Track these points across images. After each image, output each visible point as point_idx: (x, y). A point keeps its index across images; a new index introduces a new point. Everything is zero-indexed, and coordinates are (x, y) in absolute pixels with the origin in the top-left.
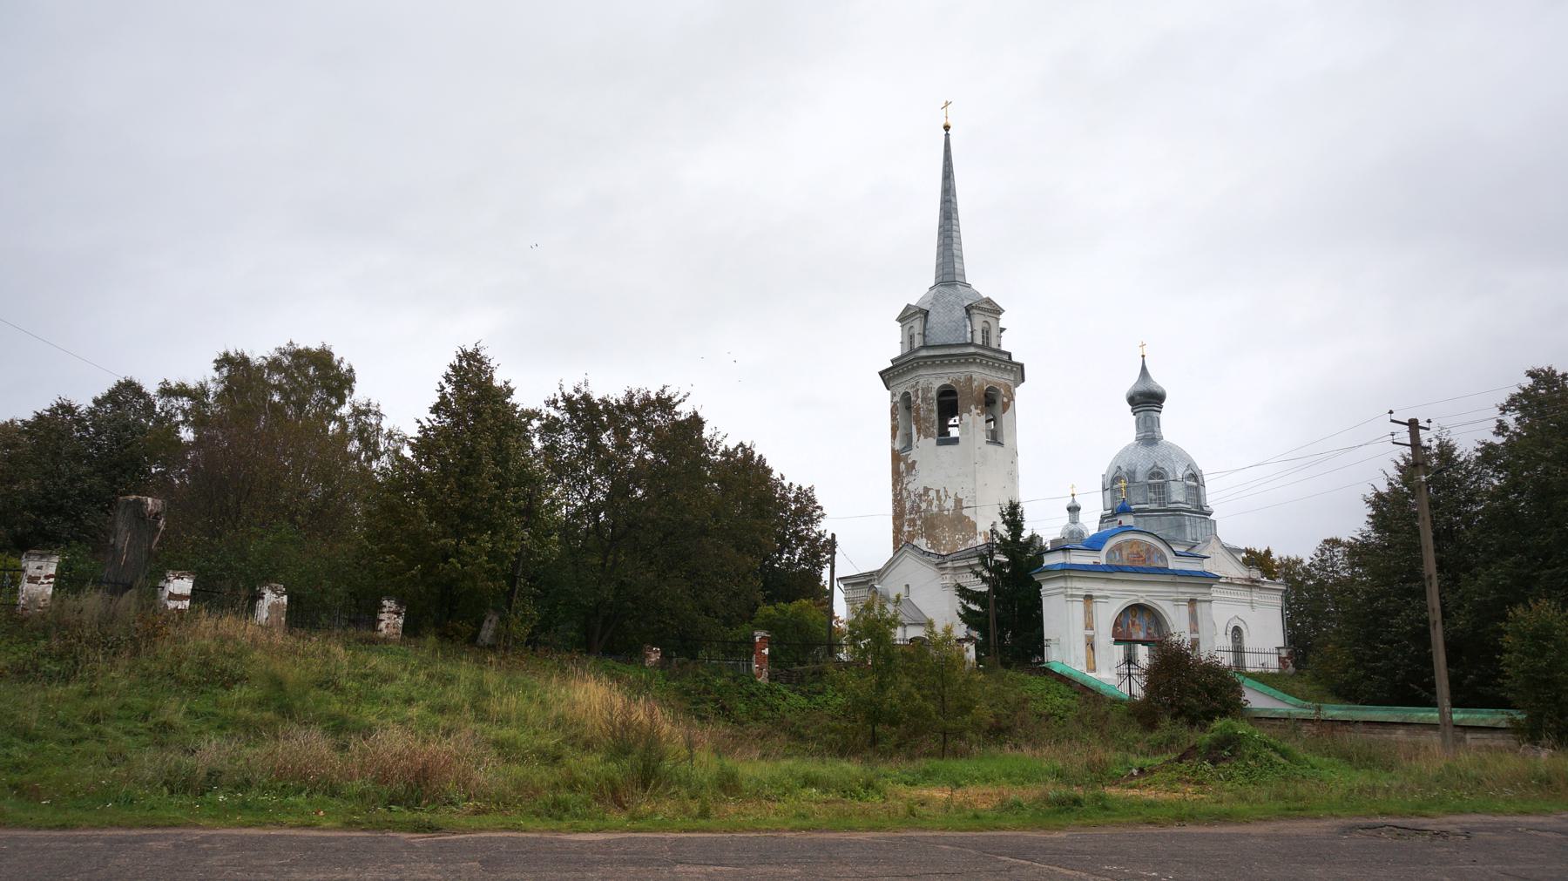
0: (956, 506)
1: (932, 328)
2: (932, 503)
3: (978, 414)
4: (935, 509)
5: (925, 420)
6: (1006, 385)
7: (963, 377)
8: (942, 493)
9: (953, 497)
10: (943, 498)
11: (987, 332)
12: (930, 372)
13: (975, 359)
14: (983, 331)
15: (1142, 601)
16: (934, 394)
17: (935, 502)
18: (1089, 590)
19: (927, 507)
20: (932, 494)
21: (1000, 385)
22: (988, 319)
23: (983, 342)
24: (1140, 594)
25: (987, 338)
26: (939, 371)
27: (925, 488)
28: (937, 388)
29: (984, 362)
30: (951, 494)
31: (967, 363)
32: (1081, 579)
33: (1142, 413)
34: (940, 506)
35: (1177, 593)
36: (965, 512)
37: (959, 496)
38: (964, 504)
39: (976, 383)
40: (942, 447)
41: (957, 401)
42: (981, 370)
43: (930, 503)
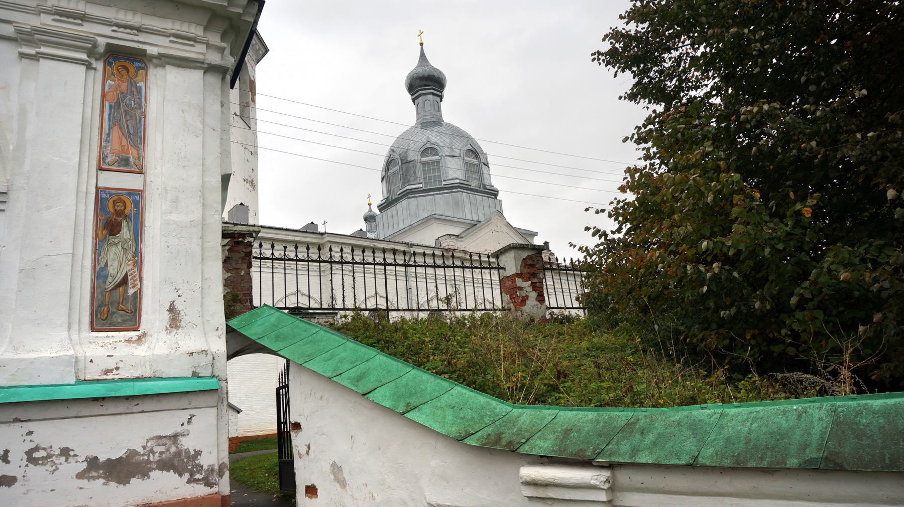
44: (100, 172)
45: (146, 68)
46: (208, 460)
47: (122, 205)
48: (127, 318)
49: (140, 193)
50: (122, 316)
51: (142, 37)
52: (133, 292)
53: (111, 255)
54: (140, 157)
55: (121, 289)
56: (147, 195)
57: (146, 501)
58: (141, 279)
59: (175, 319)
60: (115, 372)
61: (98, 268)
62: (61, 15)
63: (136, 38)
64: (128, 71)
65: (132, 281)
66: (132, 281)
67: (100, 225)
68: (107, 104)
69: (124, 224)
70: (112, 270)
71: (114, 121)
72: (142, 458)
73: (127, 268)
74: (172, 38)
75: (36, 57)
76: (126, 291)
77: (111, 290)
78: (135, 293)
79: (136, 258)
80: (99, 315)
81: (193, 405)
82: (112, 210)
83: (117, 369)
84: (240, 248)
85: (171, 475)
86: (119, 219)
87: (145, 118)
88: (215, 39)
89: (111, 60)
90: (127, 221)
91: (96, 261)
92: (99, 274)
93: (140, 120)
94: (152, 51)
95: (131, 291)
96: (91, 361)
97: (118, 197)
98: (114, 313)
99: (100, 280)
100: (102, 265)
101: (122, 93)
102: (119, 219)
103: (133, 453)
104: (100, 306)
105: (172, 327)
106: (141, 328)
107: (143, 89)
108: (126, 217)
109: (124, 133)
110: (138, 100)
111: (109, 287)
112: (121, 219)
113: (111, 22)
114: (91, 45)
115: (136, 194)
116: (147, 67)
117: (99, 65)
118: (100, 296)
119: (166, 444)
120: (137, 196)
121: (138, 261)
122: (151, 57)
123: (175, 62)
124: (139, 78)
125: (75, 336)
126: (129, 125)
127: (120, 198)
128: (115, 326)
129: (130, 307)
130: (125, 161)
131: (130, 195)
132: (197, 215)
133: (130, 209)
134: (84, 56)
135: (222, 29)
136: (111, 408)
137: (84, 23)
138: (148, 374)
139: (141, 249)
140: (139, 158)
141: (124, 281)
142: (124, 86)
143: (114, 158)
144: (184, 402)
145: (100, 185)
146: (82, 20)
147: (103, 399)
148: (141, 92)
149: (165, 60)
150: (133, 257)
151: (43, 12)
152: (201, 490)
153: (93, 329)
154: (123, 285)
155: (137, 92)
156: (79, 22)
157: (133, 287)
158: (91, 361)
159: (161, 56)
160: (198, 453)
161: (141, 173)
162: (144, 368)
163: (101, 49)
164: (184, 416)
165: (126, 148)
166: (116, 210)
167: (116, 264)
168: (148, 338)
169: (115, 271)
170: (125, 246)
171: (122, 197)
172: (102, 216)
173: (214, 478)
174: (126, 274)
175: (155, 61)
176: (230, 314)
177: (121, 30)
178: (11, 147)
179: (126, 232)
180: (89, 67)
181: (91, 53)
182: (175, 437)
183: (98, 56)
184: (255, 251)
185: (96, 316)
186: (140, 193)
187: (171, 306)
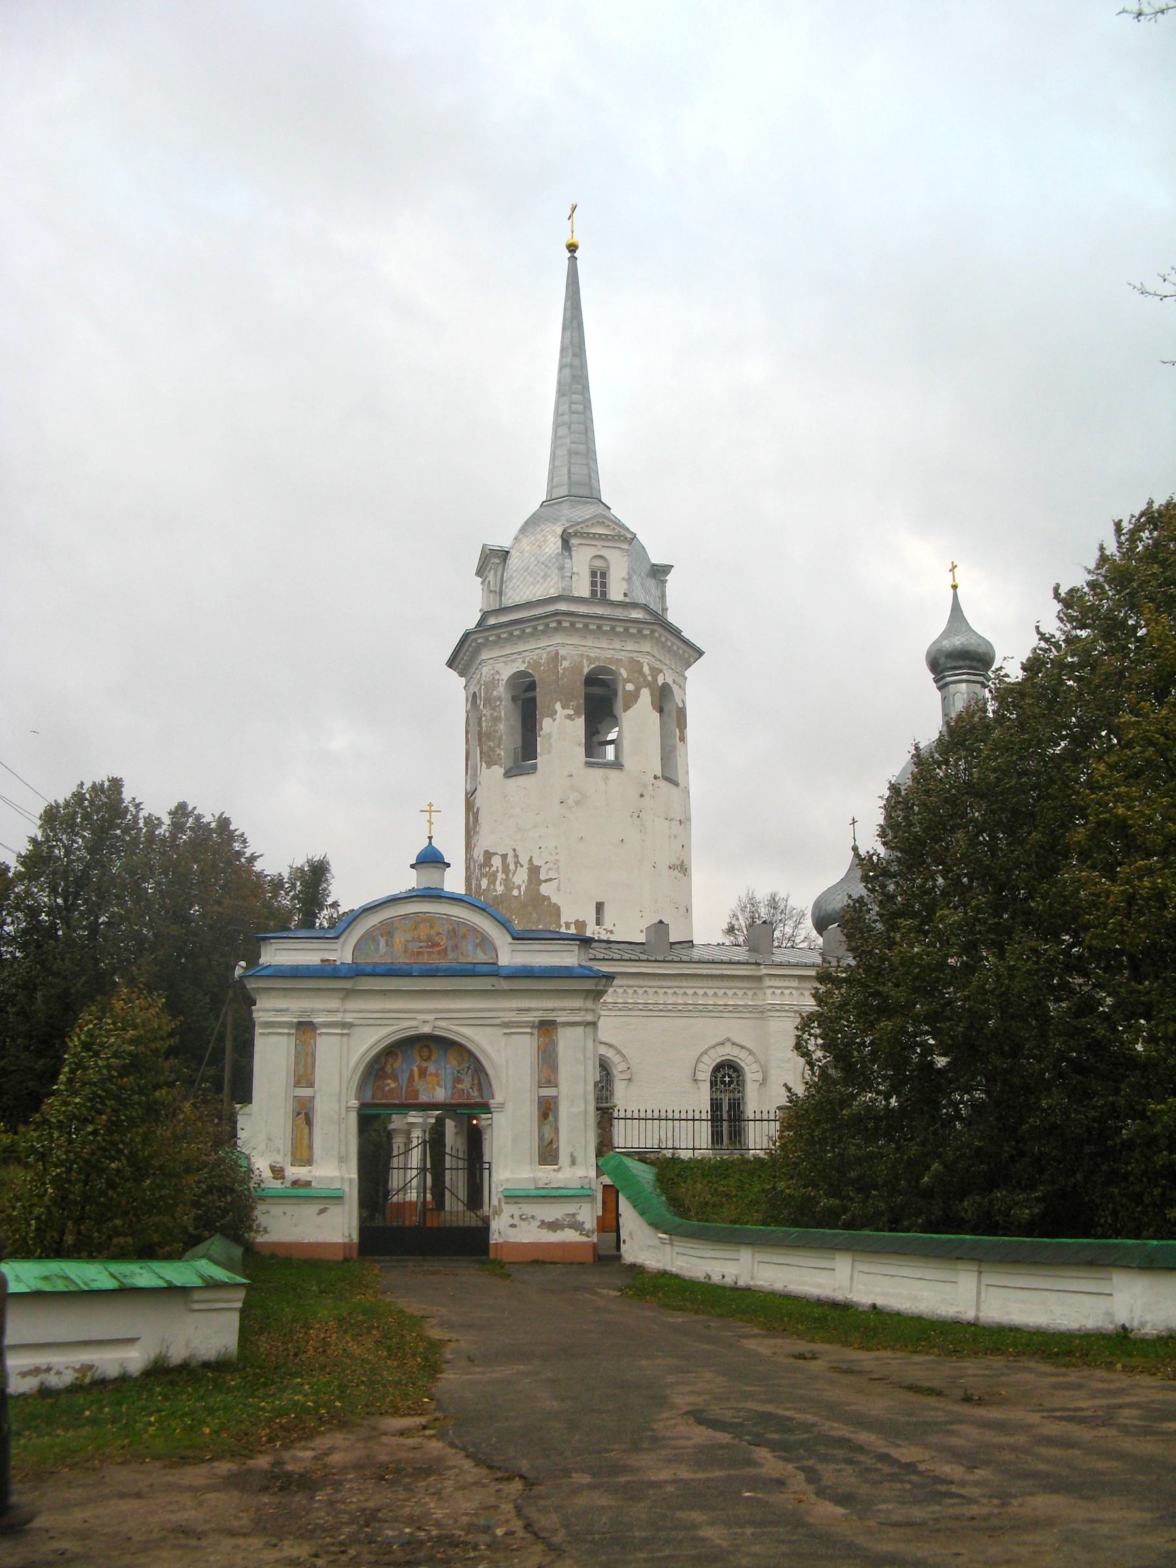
0: (530, 880)
1: (511, 578)
2: (495, 878)
3: (569, 717)
4: (500, 889)
5: (489, 736)
6: (632, 660)
7: (545, 656)
8: (510, 859)
9: (526, 865)
10: (512, 867)
11: (603, 575)
13: (559, 622)
14: (593, 574)
15: (427, 1029)
16: (501, 690)
17: (501, 876)
19: (489, 885)
20: (496, 862)
21: (618, 661)
22: (604, 552)
23: (594, 593)
24: (419, 1016)
25: (604, 585)
27: (487, 852)
28: (506, 679)
29: (541, 628)
30: (524, 860)
31: (547, 631)
33: (964, 685)
34: (507, 883)
36: (544, 889)
37: (536, 862)
38: (543, 876)
39: (566, 664)
40: (514, 779)
41: (534, 699)
42: (575, 640)
43: (492, 878)
46: (588, 1226)
70: (546, 1136)
73: (552, 1135)
84: (606, 1115)
85: (573, 1230)
92: (541, 1138)
103: (557, 1220)
106: (560, 1163)
132: (582, 1108)
133: (553, 1106)
136: (548, 1200)
141: (551, 1142)
144: (577, 1200)
152: (585, 1239)
160: (583, 1223)
164: (578, 1206)
173: (590, 1234)
176: (599, 1154)
179: (551, 1118)
182: (574, 1215)
184: (615, 1115)
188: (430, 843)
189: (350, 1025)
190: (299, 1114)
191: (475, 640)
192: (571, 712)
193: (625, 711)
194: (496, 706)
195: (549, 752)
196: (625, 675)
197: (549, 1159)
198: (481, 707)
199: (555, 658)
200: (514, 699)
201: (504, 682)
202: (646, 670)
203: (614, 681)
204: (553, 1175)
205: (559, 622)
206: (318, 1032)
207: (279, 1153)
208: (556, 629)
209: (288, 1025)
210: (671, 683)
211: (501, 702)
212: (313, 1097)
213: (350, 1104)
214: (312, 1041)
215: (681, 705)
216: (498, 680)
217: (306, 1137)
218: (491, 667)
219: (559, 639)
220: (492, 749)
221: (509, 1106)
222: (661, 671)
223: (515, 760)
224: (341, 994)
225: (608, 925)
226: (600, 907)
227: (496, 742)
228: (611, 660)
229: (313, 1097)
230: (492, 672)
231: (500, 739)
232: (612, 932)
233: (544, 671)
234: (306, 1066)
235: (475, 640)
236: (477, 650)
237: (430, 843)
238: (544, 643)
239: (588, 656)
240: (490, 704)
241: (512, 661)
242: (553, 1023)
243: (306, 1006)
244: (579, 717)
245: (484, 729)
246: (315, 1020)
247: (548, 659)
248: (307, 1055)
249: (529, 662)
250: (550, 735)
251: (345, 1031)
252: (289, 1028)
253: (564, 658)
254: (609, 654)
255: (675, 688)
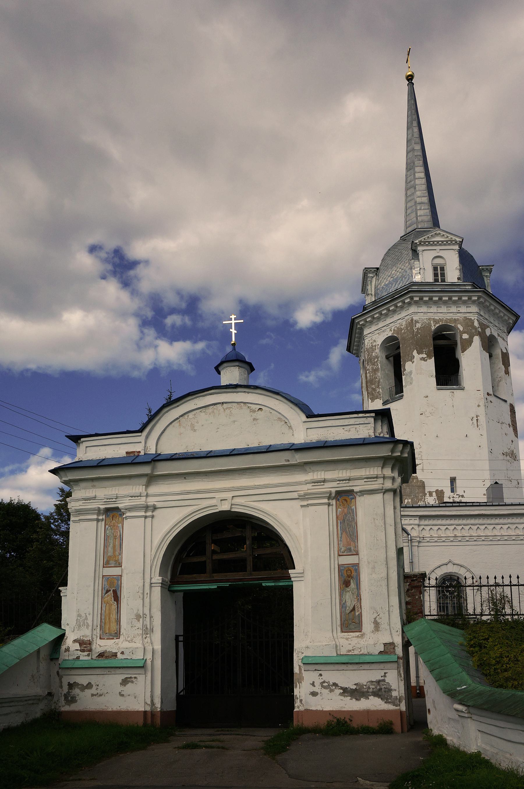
3: (423, 359)
6: (466, 319)
7: (404, 323)
12: (374, 328)
13: (412, 298)
15: (225, 507)
18: (109, 499)
21: (455, 321)
26: (381, 324)
31: (405, 306)
32: (96, 483)
35: (307, 483)
39: (418, 325)
42: (424, 309)
44: (339, 557)
45: (355, 498)
47: (350, 572)
48: (356, 626)
49: (357, 565)
50: (354, 625)
51: (351, 483)
52: (358, 614)
53: (347, 597)
54: (356, 547)
55: (353, 612)
56: (360, 565)
57: (368, 709)
58: (361, 606)
59: (377, 625)
60: (352, 651)
61: (342, 603)
62: (315, 483)
63: (348, 485)
64: (347, 501)
65: (357, 608)
66: (357, 608)
67: (342, 583)
68: (339, 521)
69: (352, 581)
70: (348, 604)
71: (343, 530)
72: (365, 690)
73: (354, 603)
74: (365, 480)
75: (308, 505)
76: (355, 614)
77: (348, 613)
78: (359, 614)
79: (358, 598)
80: (344, 625)
81: (386, 668)
82: (346, 575)
83: (353, 650)
86: (349, 579)
87: (357, 525)
88: (388, 472)
89: (339, 498)
90: (352, 580)
91: (341, 600)
92: (343, 605)
93: (354, 526)
94: (356, 489)
95: (357, 614)
96: (342, 646)
97: (347, 568)
98: (351, 624)
99: (344, 609)
100: (344, 602)
101: (345, 514)
102: (349, 579)
104: (344, 621)
105: (376, 631)
107: (355, 510)
108: (352, 577)
109: (348, 535)
110: (353, 516)
111: (348, 612)
112: (350, 579)
113: (336, 480)
114: (329, 495)
115: (355, 566)
116: (356, 497)
117: (334, 502)
118: (344, 617)
119: (375, 685)
120: (356, 567)
121: (359, 599)
122: (357, 493)
123: (367, 492)
124: (352, 504)
125: (335, 635)
126: (350, 530)
127: (349, 569)
128: (351, 630)
129: (357, 621)
130: (350, 550)
131: (353, 566)
133: (354, 574)
134: (326, 501)
135: (391, 465)
137: (325, 484)
138: (366, 653)
139: (360, 593)
140: (356, 548)
141: (354, 609)
142: (346, 510)
143: (344, 548)
145: (340, 563)
146: (323, 482)
147: (347, 663)
148: (354, 512)
149: (363, 493)
150: (357, 597)
151: (307, 483)
153: (342, 632)
154: (353, 610)
155: (352, 512)
156: (323, 484)
157: (358, 611)
158: (342, 646)
159: (360, 492)
161: (357, 554)
162: (364, 650)
163: (333, 495)
165: (349, 543)
166: (347, 575)
167: (349, 601)
168: (366, 636)
169: (350, 604)
170: (353, 592)
171: (350, 568)
172: (342, 578)
174: (354, 605)
175: (358, 494)
177: (341, 482)
178: (303, 551)
179: (353, 585)
180: (329, 505)
181: (329, 498)
183: (332, 498)
185: (343, 625)
186: (357, 565)
187: (374, 620)
188: (234, 349)
189: (155, 508)
190: (108, 591)
191: (358, 323)
192: (424, 356)
193: (463, 352)
194: (375, 362)
195: (411, 383)
196: (461, 328)
197: (352, 626)
198: (366, 366)
199: (412, 323)
200: (387, 358)
201: (379, 346)
202: (476, 324)
203: (454, 335)
204: (354, 641)
205: (412, 298)
206: (124, 516)
207: (87, 628)
208: (409, 304)
209: (99, 511)
210: (496, 336)
211: (378, 358)
212: (121, 576)
213: (153, 581)
214: (120, 525)
215: (505, 351)
216: (375, 346)
217: (114, 612)
218: (370, 339)
219: (413, 309)
220: (374, 390)
221: (308, 575)
222: (488, 327)
223: (391, 395)
224: (144, 480)
225: (459, 491)
226: (453, 480)
227: (377, 384)
228: (450, 320)
229: (121, 576)
230: (371, 341)
231: (379, 382)
232: (463, 496)
233: (404, 333)
234: (114, 547)
235: (358, 323)
236: (362, 330)
237: (234, 349)
238: (404, 314)
239: (434, 319)
240: (371, 362)
241: (383, 331)
242: (349, 493)
243: (113, 493)
244: (430, 358)
245: (368, 378)
246: (120, 506)
247: (406, 325)
248: (115, 538)
249: (394, 330)
250: (411, 372)
251: (149, 514)
252: (99, 514)
253: (417, 322)
254: (449, 316)
255: (500, 340)
